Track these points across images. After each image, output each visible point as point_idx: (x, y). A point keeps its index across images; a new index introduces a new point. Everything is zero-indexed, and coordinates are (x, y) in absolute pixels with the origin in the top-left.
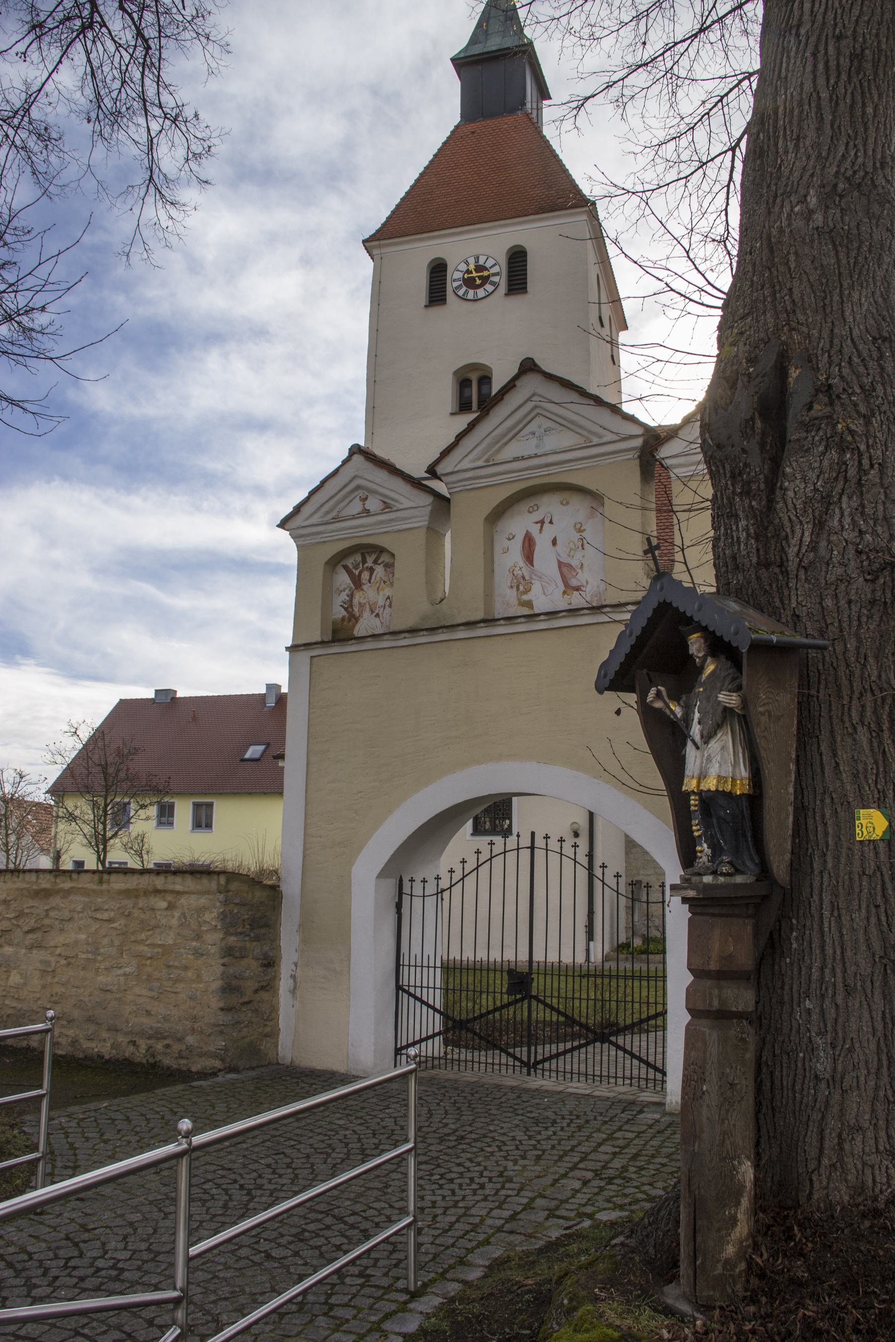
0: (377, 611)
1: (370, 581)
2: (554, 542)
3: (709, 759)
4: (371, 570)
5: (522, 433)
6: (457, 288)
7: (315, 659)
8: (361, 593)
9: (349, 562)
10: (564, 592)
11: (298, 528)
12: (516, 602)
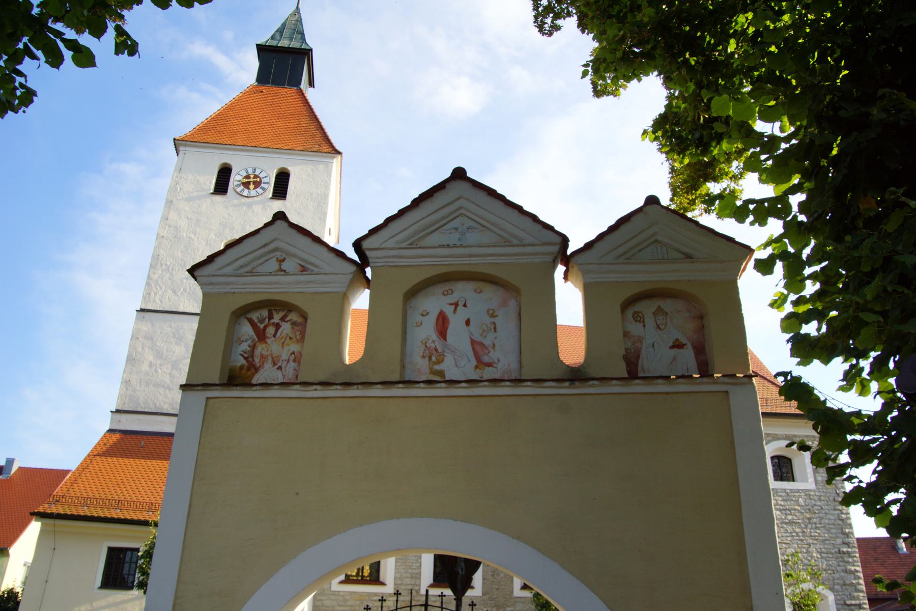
0: (279, 364)
1: (275, 336)
2: (468, 323)
4: (278, 326)
5: (445, 227)
6: (236, 186)
7: (211, 401)
8: (264, 346)
9: (255, 316)
10: (476, 367)
11: (209, 276)
12: (428, 371)
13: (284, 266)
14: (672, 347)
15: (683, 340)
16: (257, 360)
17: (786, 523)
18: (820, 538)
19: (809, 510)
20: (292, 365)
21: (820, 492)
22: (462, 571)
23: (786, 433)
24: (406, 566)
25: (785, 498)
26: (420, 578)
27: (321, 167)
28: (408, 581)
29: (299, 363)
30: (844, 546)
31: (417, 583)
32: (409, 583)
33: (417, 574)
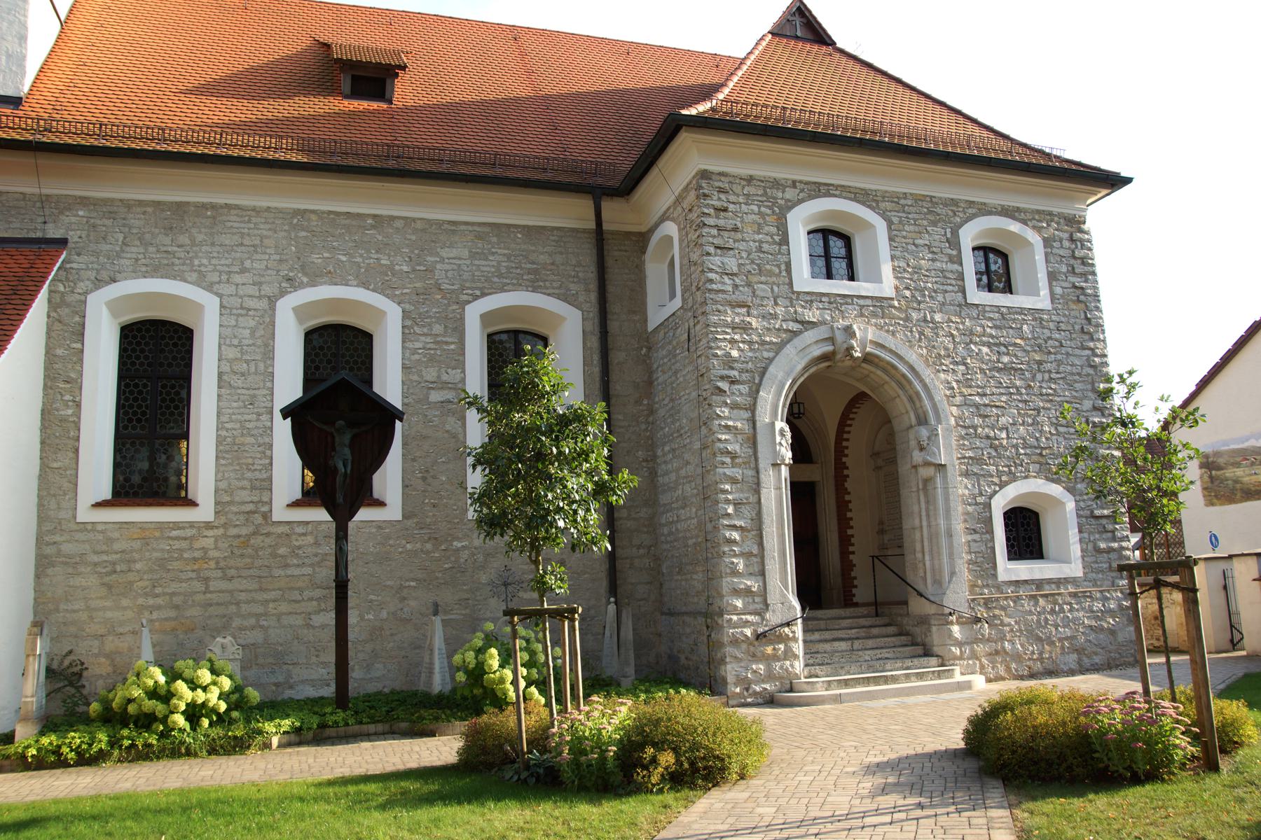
17: (999, 370)
18: (1056, 398)
19: (1039, 346)
21: (1058, 314)
22: (345, 466)
23: (1002, 203)
24: (239, 464)
25: (998, 323)
26: (271, 490)
28: (244, 495)
30: (1094, 413)
31: (265, 499)
32: (250, 499)
33: (264, 480)
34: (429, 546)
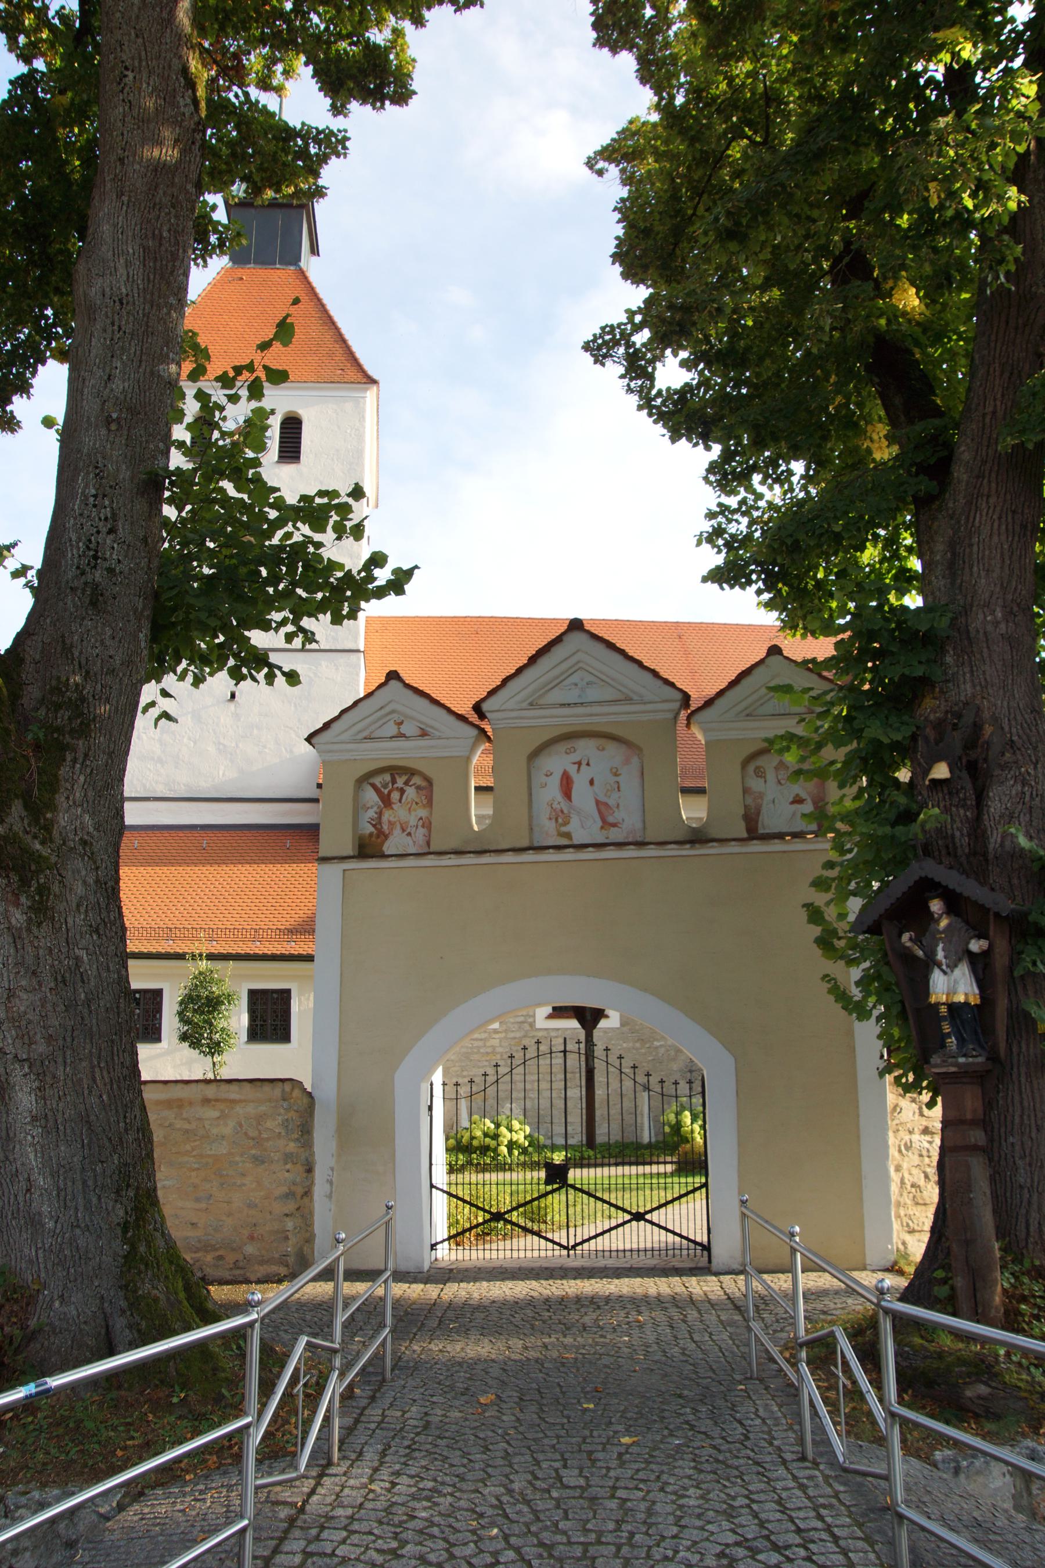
2: (592, 782)
3: (956, 982)
4: (402, 791)
5: (565, 683)
9: (377, 781)
13: (404, 729)
14: (792, 803)
15: (803, 795)
16: (385, 827)
20: (421, 831)
27: (349, 406)
29: (430, 831)
34: (638, 1045)
